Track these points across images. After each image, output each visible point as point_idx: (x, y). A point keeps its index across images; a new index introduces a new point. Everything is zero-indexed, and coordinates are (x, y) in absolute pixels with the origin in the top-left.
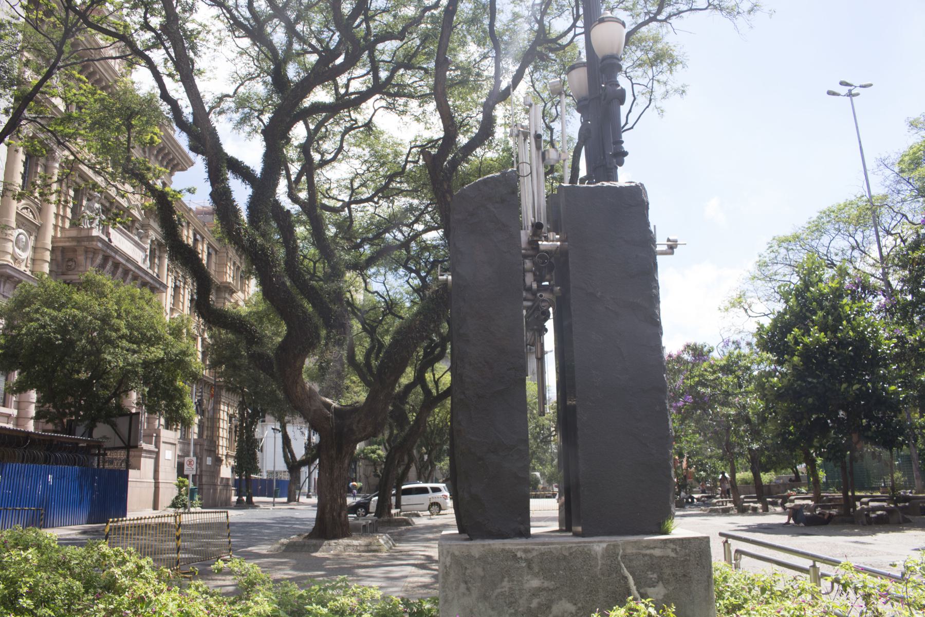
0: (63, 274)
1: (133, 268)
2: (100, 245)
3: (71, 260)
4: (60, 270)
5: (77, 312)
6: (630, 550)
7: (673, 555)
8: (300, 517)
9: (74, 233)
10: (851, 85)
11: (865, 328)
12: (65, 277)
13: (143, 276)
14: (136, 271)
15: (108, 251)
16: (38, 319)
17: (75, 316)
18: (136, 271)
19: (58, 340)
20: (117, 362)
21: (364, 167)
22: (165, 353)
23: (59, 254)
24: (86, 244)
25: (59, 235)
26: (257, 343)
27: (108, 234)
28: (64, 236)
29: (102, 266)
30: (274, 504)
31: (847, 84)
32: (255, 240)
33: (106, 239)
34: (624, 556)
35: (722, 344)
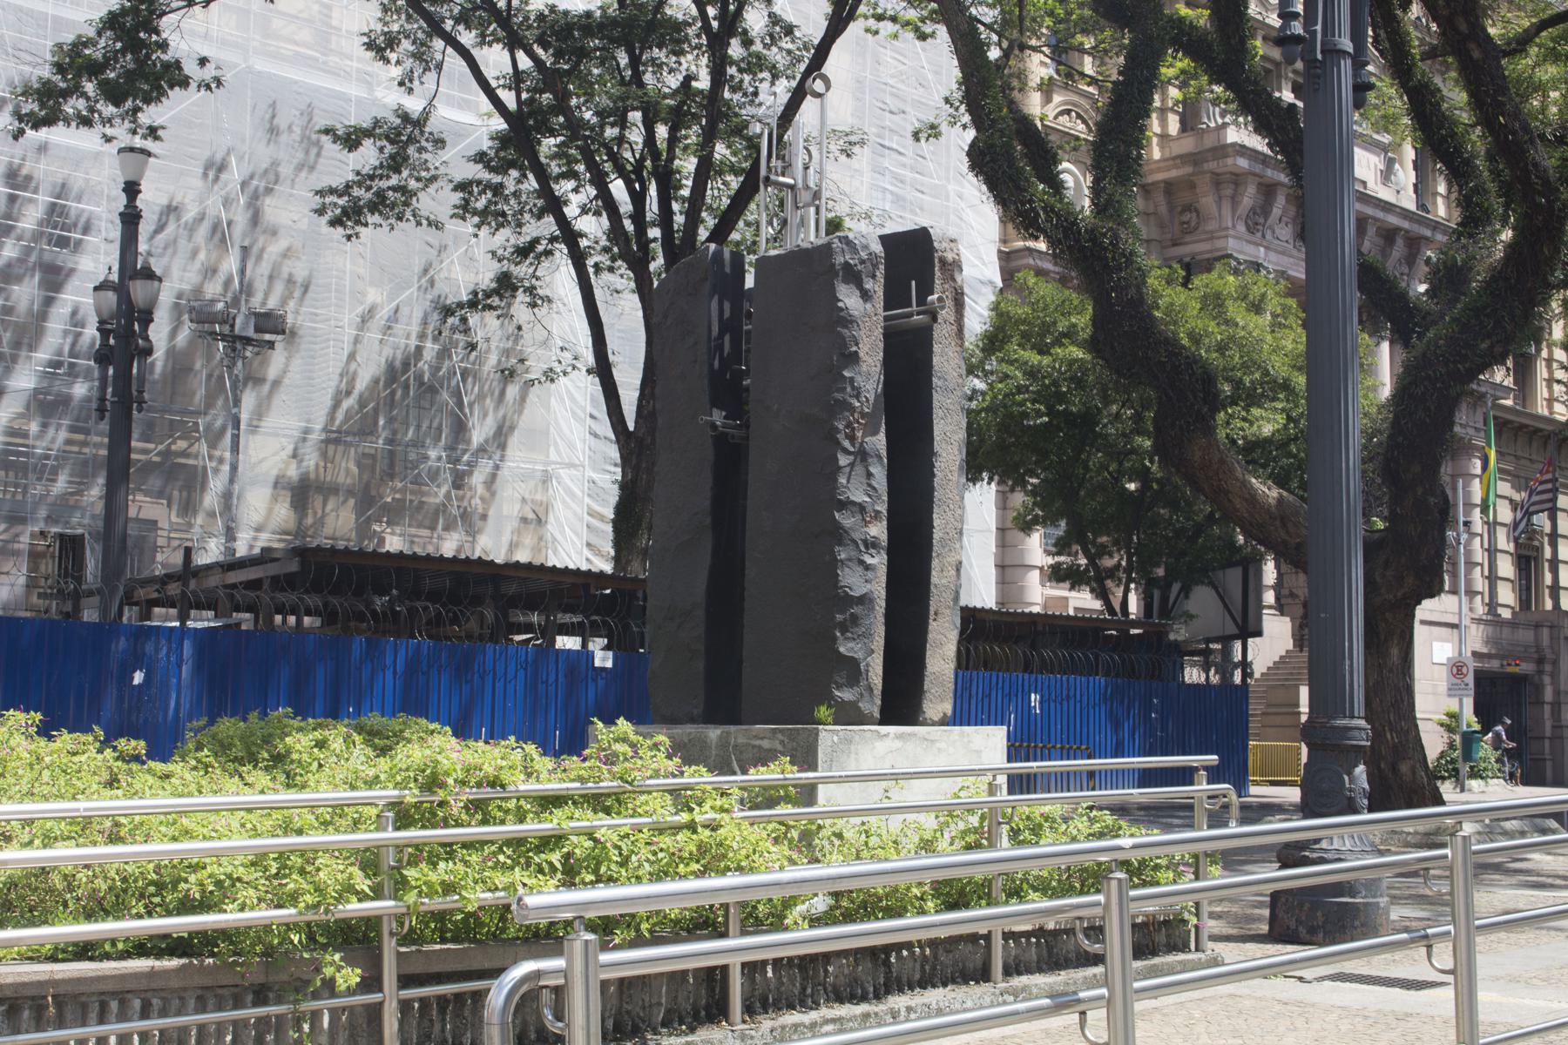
2: (1243, 163)
4: (1169, 236)
6: (741, 740)
9: (1188, 145)
13: (1380, 215)
15: (1269, 172)
19: (1039, 414)
22: (1289, 419)
23: (1160, 198)
24: (1212, 165)
28: (1167, 155)
34: (736, 746)
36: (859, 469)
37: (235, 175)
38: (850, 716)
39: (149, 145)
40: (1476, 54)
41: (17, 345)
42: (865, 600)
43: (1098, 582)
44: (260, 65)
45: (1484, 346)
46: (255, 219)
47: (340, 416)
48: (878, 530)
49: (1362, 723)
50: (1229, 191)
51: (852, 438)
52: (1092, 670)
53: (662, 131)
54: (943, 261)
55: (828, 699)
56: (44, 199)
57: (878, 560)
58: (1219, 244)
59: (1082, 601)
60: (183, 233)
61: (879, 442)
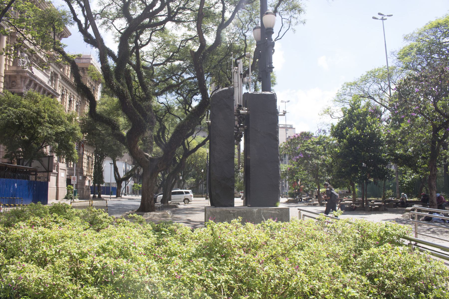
0: (10, 88)
1: (43, 86)
2: (28, 75)
3: (14, 81)
5: (25, 110)
6: (265, 211)
7: (278, 213)
8: (125, 204)
9: (15, 68)
10: (383, 15)
11: (375, 129)
12: (11, 90)
13: (49, 90)
14: (45, 87)
16: (7, 113)
17: (24, 111)
18: (45, 87)
19: (17, 122)
20: (44, 133)
21: (159, 46)
23: (8, 78)
24: (21, 74)
25: (7, 69)
26: (117, 129)
27: (31, 69)
29: (29, 84)
30: (110, 198)
31: (381, 15)
32: (119, 87)
33: (31, 72)
34: (263, 213)
35: (318, 131)
58: (21, 90)
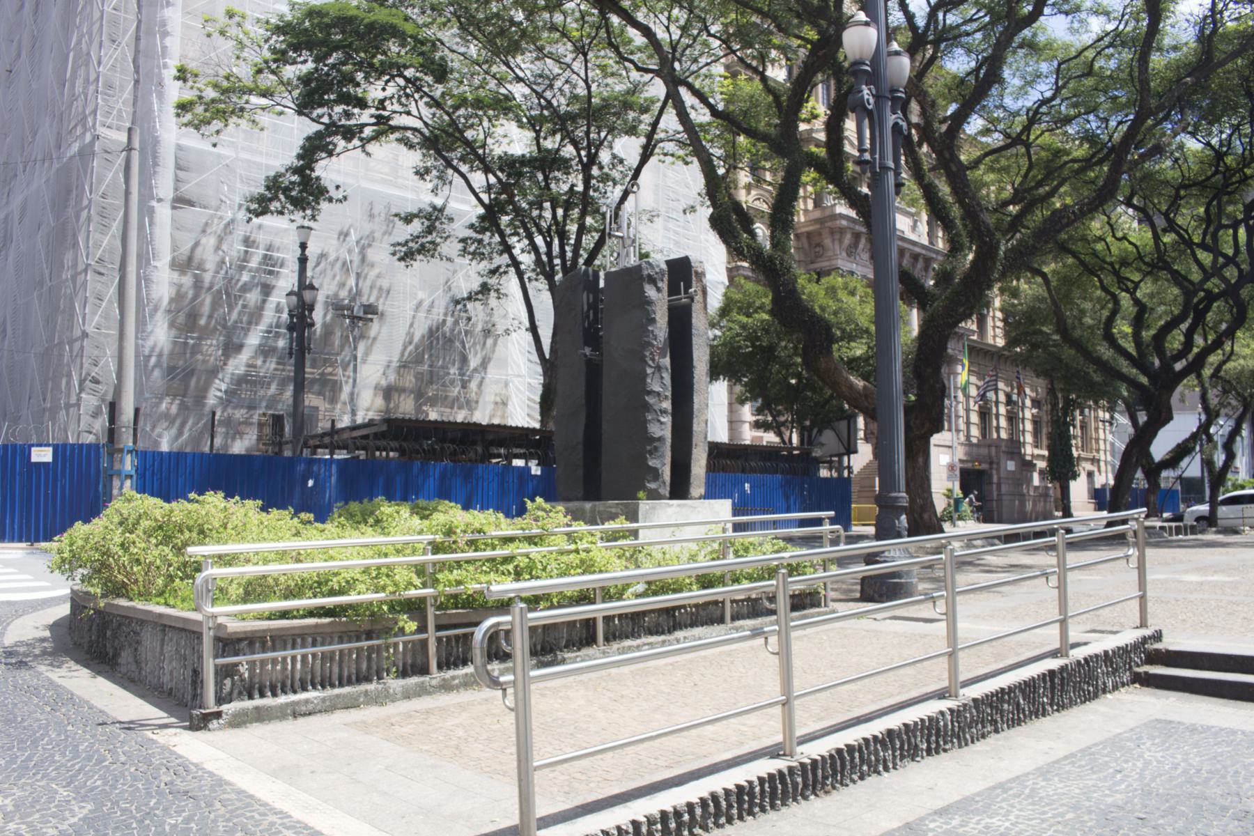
0: (813, 262)
2: (844, 223)
9: (817, 214)
13: (911, 247)
19: (747, 347)
23: (804, 240)
24: (829, 224)
36: (657, 375)
37: (353, 237)
38: (654, 495)
39: (312, 224)
40: (954, 169)
41: (250, 323)
42: (661, 439)
43: (777, 428)
44: (365, 184)
45: (961, 310)
46: (363, 259)
47: (406, 354)
48: (667, 405)
49: (904, 495)
50: (837, 236)
51: (653, 360)
52: (775, 472)
53: (560, 212)
54: (696, 273)
55: (644, 488)
56: (261, 252)
57: (667, 420)
58: (834, 262)
59: (770, 438)
60: (329, 267)
61: (666, 361)
